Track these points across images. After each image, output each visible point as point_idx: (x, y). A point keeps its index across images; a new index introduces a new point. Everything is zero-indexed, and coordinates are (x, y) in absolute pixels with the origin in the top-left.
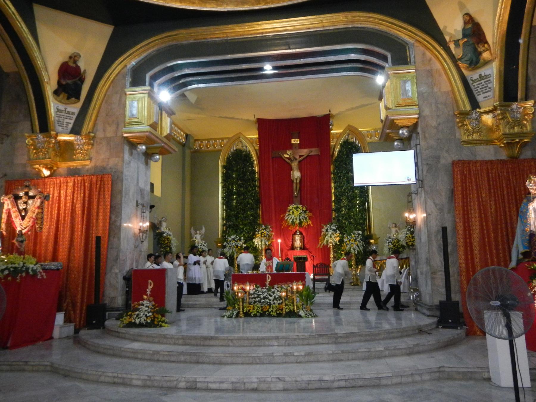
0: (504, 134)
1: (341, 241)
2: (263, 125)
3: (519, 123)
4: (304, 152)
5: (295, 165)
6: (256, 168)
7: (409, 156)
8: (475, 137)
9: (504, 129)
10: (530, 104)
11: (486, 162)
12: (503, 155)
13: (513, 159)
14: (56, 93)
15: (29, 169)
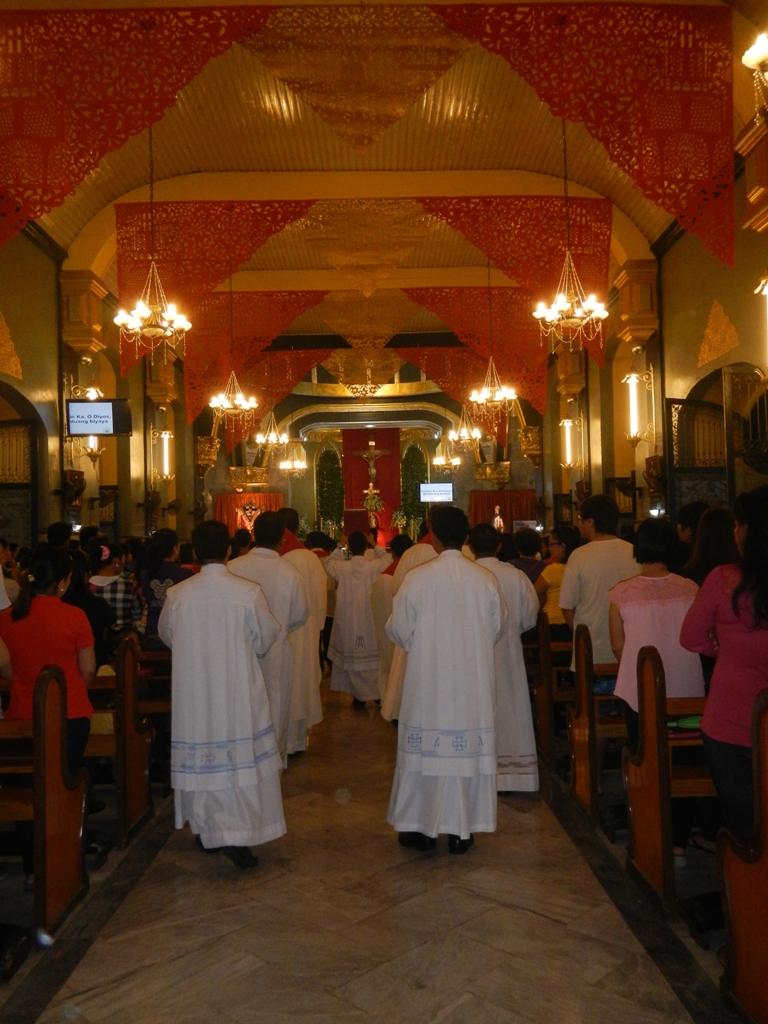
0: (497, 479)
1: (408, 524)
2: (346, 433)
3: (502, 472)
4: (378, 452)
5: (372, 463)
6: (341, 465)
7: (449, 487)
8: (484, 477)
9: (496, 476)
10: (508, 463)
11: (487, 492)
12: (496, 488)
13: (501, 489)
14: (248, 443)
15: (227, 486)
